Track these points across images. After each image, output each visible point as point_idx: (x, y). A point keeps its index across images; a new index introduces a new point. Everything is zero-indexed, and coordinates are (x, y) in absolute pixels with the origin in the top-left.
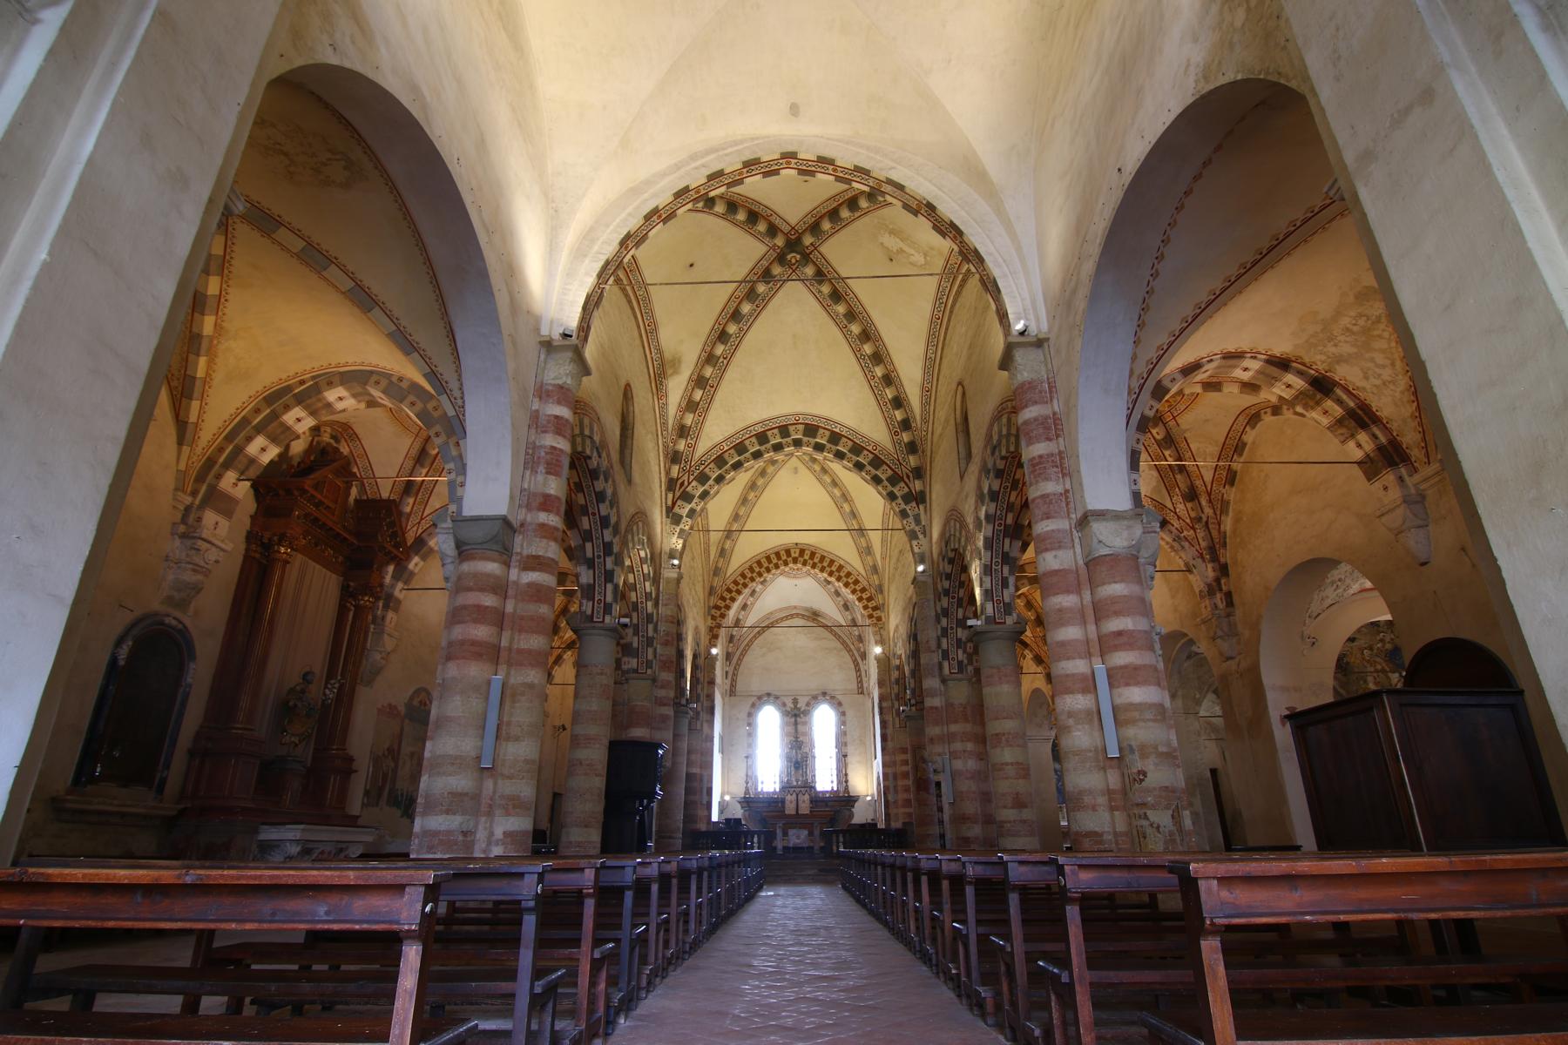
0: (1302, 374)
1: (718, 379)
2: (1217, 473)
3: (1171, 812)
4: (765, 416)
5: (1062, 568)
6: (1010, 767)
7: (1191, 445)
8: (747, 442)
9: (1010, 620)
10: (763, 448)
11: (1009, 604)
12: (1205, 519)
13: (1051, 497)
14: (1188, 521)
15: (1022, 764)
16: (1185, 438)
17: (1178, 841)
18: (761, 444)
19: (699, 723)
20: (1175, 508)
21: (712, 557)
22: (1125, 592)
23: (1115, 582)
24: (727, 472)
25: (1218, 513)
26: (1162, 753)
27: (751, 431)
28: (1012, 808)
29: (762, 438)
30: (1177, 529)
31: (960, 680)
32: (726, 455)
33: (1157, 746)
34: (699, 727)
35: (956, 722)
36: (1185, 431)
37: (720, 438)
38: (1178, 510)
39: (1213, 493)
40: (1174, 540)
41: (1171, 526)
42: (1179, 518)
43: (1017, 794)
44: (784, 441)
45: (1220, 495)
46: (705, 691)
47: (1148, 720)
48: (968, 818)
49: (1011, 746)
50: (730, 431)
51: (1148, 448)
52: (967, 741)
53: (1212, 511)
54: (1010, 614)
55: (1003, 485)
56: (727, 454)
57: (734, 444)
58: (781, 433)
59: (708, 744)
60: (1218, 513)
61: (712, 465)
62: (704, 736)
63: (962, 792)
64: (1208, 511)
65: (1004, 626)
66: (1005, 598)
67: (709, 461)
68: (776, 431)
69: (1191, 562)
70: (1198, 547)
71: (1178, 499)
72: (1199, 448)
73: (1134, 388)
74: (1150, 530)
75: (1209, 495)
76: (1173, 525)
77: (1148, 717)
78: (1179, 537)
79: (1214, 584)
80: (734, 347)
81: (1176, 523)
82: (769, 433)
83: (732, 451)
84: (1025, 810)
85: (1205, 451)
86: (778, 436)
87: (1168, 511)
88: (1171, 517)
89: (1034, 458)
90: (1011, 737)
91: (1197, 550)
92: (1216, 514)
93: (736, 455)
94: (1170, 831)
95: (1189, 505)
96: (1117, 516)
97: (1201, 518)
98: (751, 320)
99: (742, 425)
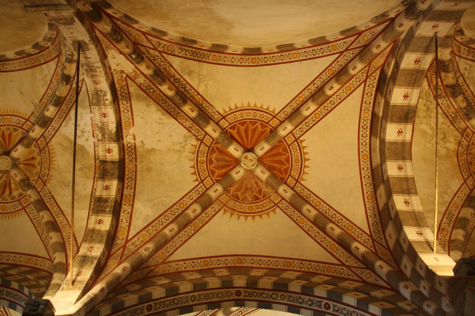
7: (43, 94)
16: (40, 102)
36: (35, 105)
51: (56, 129)
55: (5, 297)
85: (42, 79)
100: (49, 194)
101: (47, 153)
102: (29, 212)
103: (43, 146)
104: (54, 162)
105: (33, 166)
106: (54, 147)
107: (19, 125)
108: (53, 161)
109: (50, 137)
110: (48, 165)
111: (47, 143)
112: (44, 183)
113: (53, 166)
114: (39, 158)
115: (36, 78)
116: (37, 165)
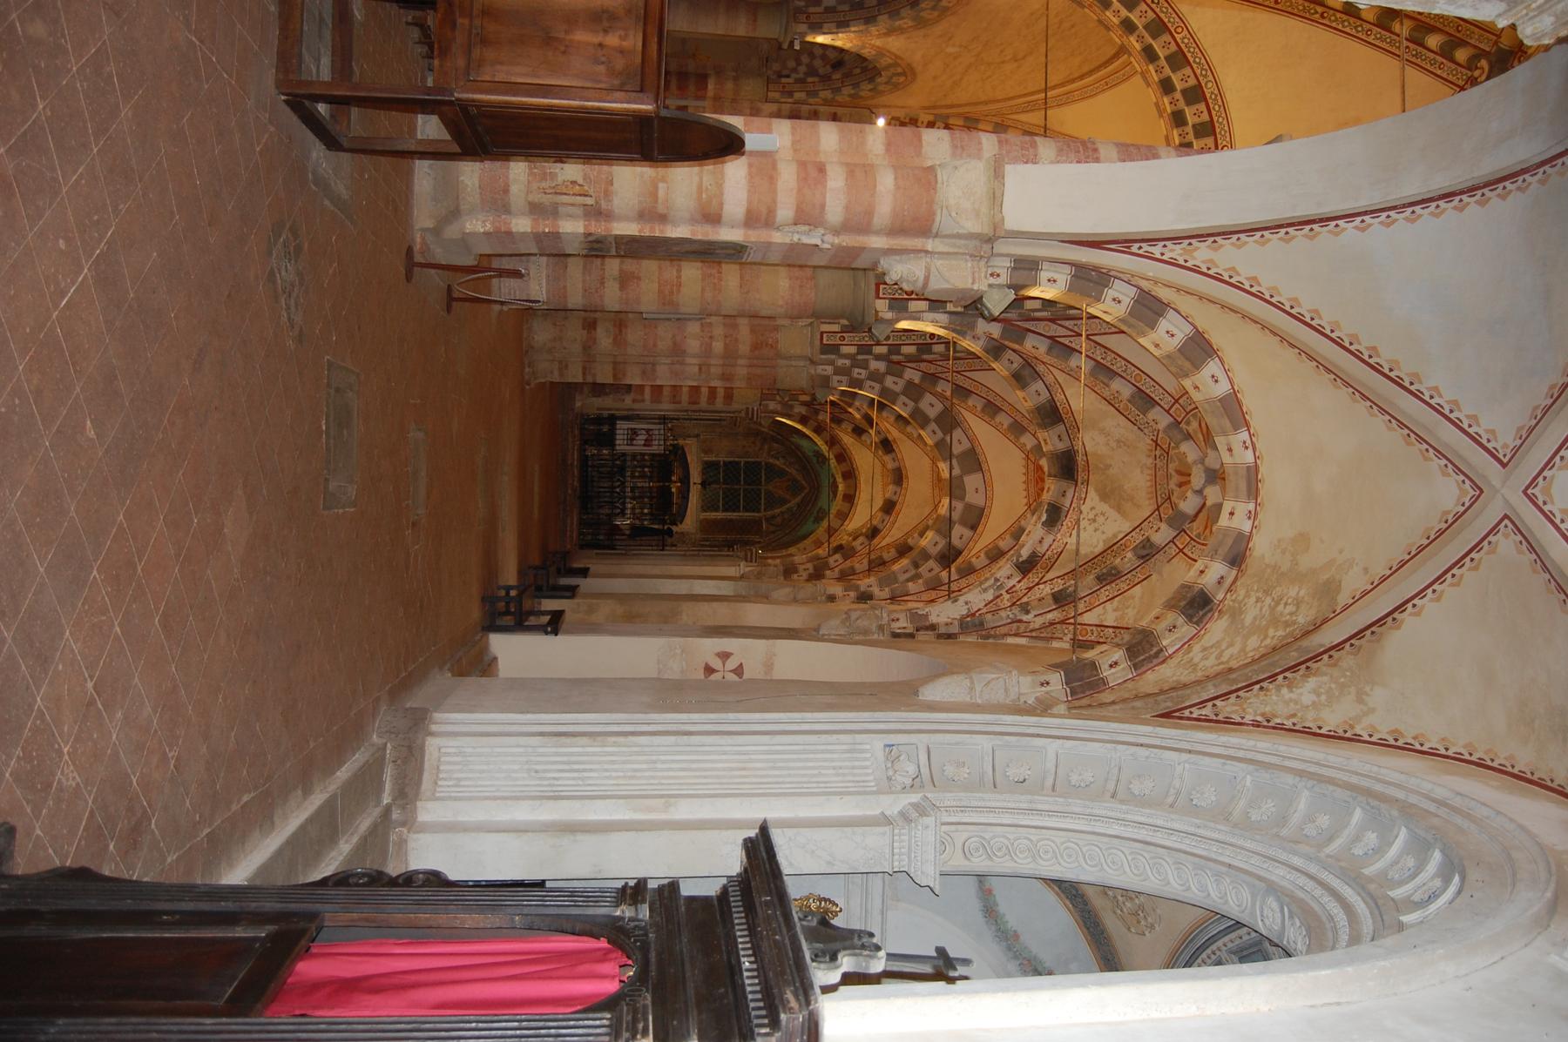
0: (1219, 583)
1: (1289, 9)
2: (1094, 628)
3: (580, 181)
4: (1231, 97)
5: (924, 142)
6: (675, 273)
8: (1187, 71)
9: (881, 305)
10: (1178, 95)
11: (906, 308)
12: (1025, 618)
13: (1031, 150)
14: (1025, 600)
15: (679, 291)
17: (543, 184)
18: (1184, 92)
19: (776, 95)
20: (1045, 582)
21: (1023, 117)
22: (880, 188)
23: (896, 179)
24: (1140, 38)
25: (1034, 634)
26: (656, 188)
27: (1205, 76)
28: (621, 270)
29: (1195, 94)
30: (1014, 586)
31: (812, 344)
32: (1166, 37)
33: (667, 182)
34: (771, 95)
35: (753, 331)
36: (1160, 573)
37: (1194, 24)
38: (1041, 586)
39: (1064, 626)
40: (997, 580)
41: (1018, 579)
42: (1030, 589)
43: (639, 278)
44: (1189, 129)
45: (1060, 636)
46: (822, 109)
47: (701, 179)
48: (621, 331)
49: (703, 280)
50: (1206, 42)
51: (1138, 530)
52: (726, 345)
53: (1037, 626)
54: (891, 308)
56: (1169, 38)
57: (1185, 50)
58: (1202, 124)
59: (748, 111)
60: (1034, 634)
61: (1151, 15)
62: (759, 104)
63: (656, 327)
64: (1039, 622)
65: (873, 292)
66: (914, 302)
67: (1158, 10)
68: (1205, 117)
69: (962, 599)
70: (984, 611)
71: (1059, 585)
72: (1133, 598)
73: (1195, 259)
74: (976, 275)
75: (1062, 622)
76: (1019, 582)
77: (705, 179)
78: (1000, 587)
79: (927, 624)
80: (1340, 27)
81: (1024, 584)
82: (1202, 107)
83: (1173, 48)
84: (617, 286)
86: (1197, 120)
87: (1040, 576)
88: (1033, 577)
89: (1094, 143)
90: (716, 281)
91: (979, 610)
92: (1032, 631)
93: (1167, 52)
94: (556, 174)
95: (1050, 600)
96: (996, 199)
97: (1028, 612)
98: (1384, 45)
99: (1214, 56)
100: (1142, 427)
101: (1159, 493)
102: (1166, 395)
103: (1166, 505)
104: (1148, 478)
105: (1179, 473)
106: (1147, 502)
107: (1194, 543)
108: (1151, 480)
109: (1151, 519)
110: (1158, 474)
111: (1158, 509)
112: (1157, 444)
113: (1150, 472)
114: (1172, 485)
115: (1138, 612)
116: (1174, 473)
